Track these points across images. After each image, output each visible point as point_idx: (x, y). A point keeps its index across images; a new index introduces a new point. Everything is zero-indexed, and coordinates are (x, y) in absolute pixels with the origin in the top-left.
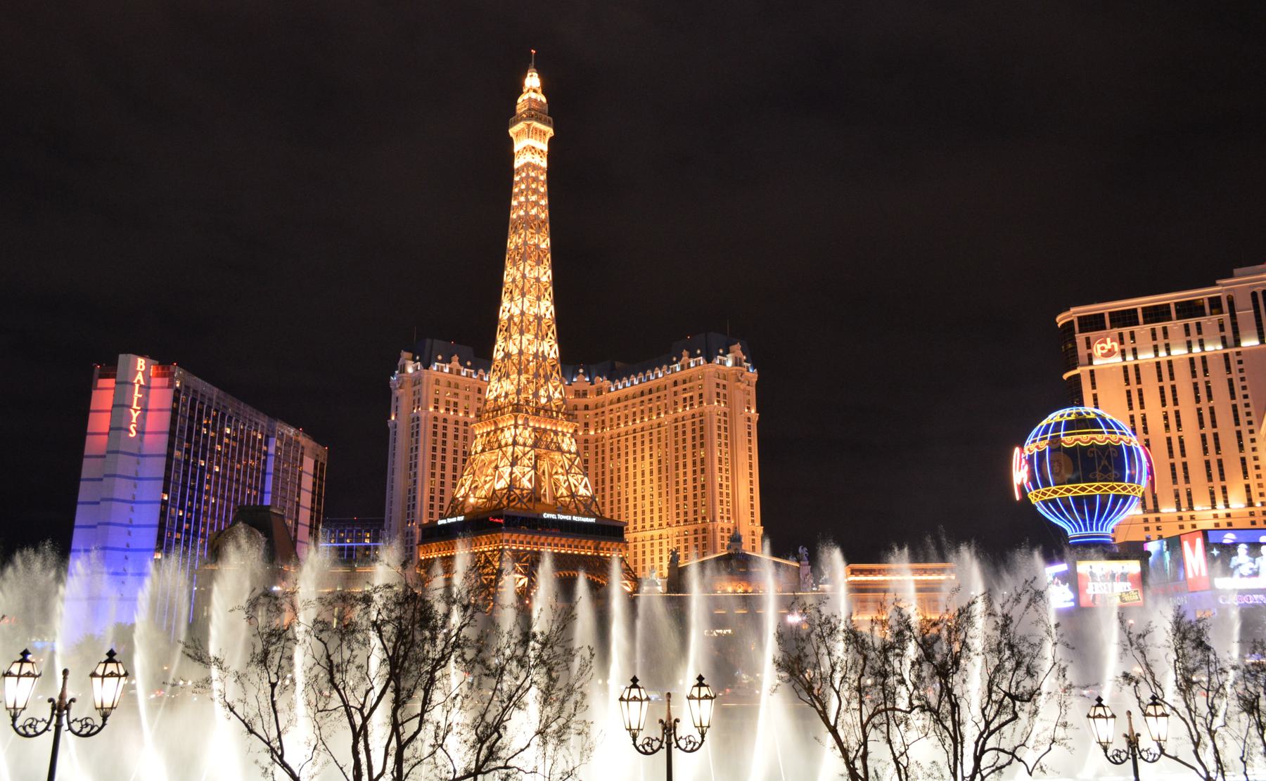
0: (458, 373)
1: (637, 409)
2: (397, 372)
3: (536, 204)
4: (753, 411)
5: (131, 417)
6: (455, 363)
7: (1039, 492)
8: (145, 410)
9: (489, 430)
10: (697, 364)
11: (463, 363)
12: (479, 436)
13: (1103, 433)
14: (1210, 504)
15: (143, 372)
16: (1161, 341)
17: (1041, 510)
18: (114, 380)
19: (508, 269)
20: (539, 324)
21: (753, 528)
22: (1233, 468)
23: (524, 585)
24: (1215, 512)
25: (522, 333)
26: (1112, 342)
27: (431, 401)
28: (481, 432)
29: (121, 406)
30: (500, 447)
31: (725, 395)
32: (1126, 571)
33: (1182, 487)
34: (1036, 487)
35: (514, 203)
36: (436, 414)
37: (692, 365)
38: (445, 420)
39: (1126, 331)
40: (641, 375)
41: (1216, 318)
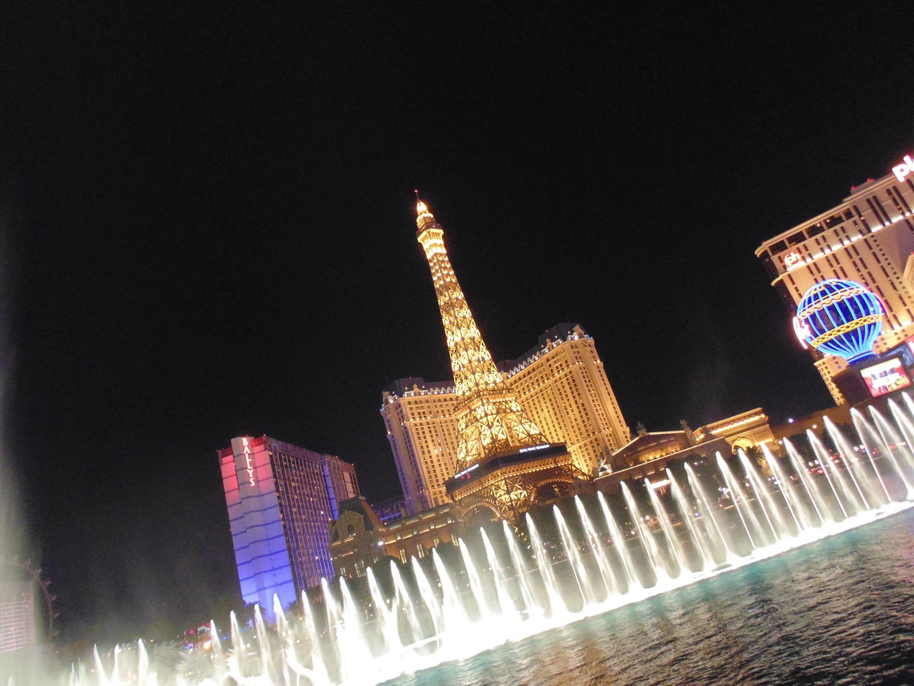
0: (420, 394)
1: (529, 383)
2: (383, 405)
3: (448, 275)
4: (599, 362)
5: (249, 474)
6: (416, 389)
8: (255, 468)
9: (466, 413)
10: (558, 344)
11: (420, 388)
12: (460, 419)
13: (846, 290)
15: (248, 446)
16: (823, 244)
18: (232, 456)
19: (444, 317)
20: (474, 342)
21: (624, 430)
23: (525, 495)
24: (894, 331)
25: (466, 350)
27: (410, 415)
28: (461, 416)
29: (240, 470)
30: (477, 420)
31: (580, 357)
35: (435, 278)
36: (415, 422)
37: (555, 346)
38: (421, 424)
39: (800, 245)
40: (524, 363)
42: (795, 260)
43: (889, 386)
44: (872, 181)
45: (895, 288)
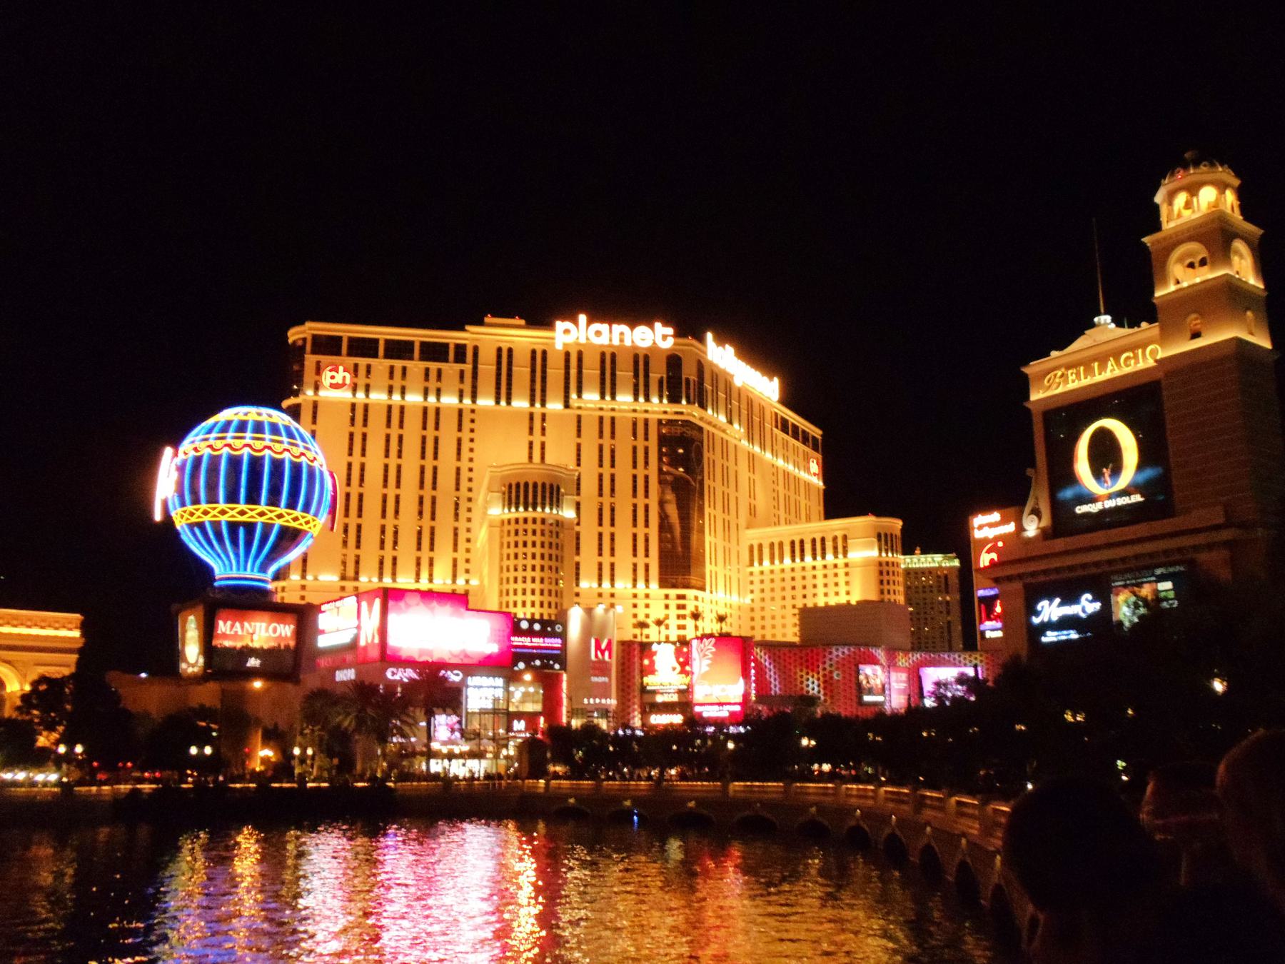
7: (185, 512)
14: (413, 576)
17: (187, 537)
22: (444, 540)
26: (344, 371)
33: (388, 553)
34: (183, 504)
39: (363, 362)
42: (340, 382)
44: (522, 322)
45: (457, 515)
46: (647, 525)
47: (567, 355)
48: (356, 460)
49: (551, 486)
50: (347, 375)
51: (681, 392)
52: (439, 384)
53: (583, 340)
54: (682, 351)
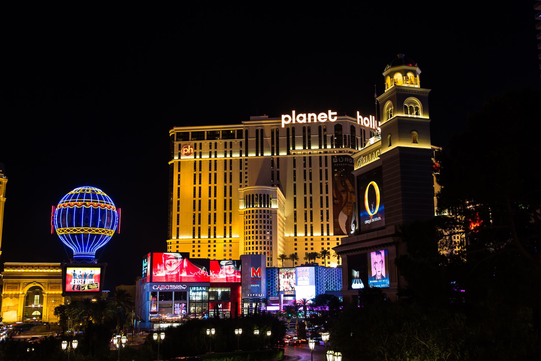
7: (60, 230)
13: (97, 202)
32: (93, 273)
39: (198, 142)
41: (239, 140)
43: (82, 287)
46: (327, 206)
47: (288, 129)
48: (197, 186)
49: (264, 195)
50: (192, 149)
51: (342, 143)
52: (231, 149)
53: (294, 122)
54: (342, 122)
